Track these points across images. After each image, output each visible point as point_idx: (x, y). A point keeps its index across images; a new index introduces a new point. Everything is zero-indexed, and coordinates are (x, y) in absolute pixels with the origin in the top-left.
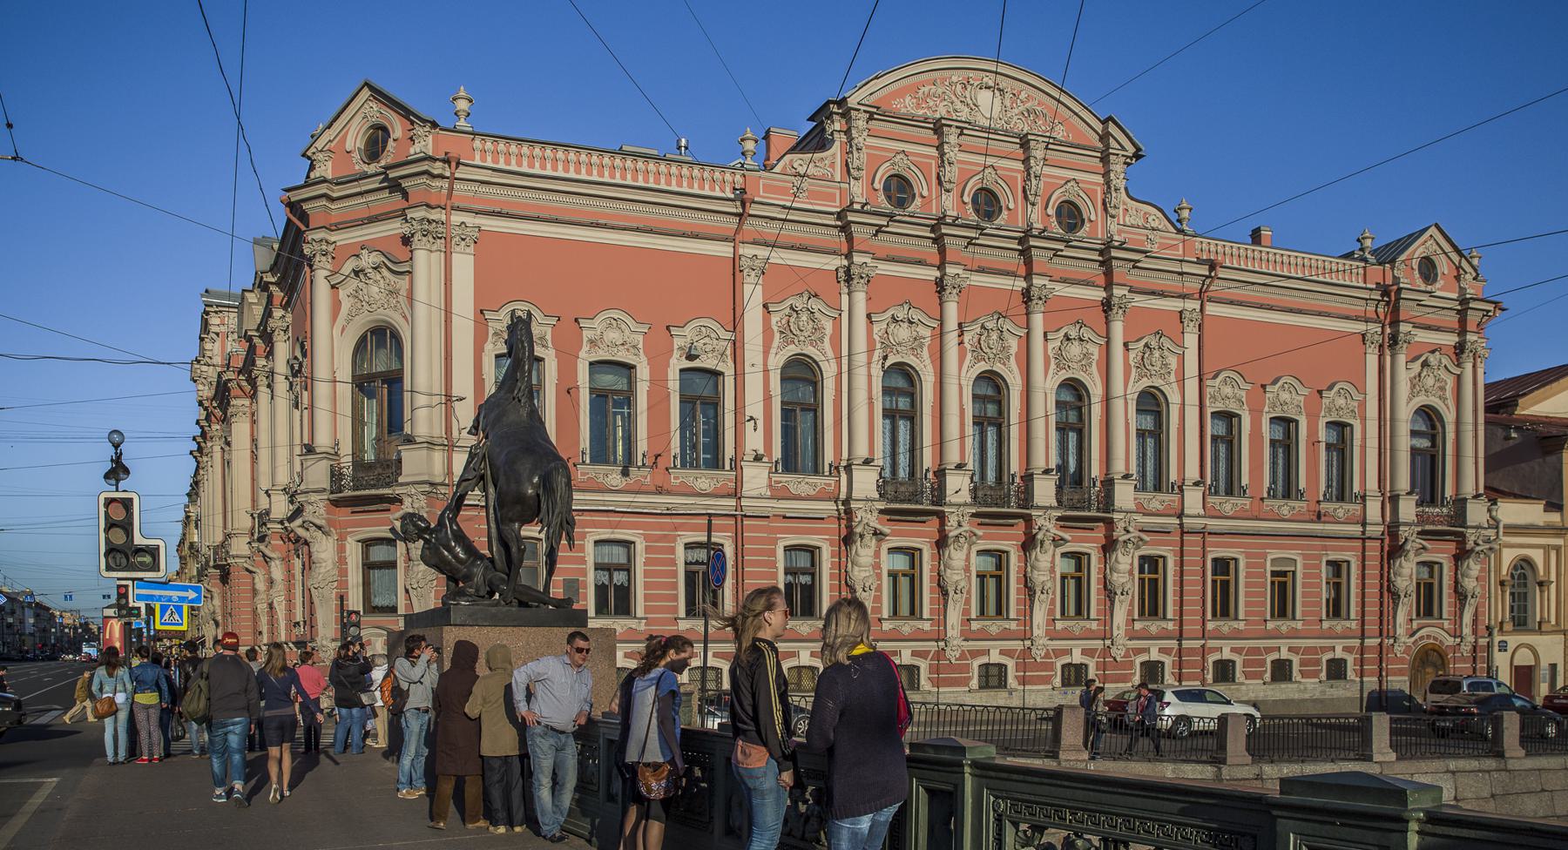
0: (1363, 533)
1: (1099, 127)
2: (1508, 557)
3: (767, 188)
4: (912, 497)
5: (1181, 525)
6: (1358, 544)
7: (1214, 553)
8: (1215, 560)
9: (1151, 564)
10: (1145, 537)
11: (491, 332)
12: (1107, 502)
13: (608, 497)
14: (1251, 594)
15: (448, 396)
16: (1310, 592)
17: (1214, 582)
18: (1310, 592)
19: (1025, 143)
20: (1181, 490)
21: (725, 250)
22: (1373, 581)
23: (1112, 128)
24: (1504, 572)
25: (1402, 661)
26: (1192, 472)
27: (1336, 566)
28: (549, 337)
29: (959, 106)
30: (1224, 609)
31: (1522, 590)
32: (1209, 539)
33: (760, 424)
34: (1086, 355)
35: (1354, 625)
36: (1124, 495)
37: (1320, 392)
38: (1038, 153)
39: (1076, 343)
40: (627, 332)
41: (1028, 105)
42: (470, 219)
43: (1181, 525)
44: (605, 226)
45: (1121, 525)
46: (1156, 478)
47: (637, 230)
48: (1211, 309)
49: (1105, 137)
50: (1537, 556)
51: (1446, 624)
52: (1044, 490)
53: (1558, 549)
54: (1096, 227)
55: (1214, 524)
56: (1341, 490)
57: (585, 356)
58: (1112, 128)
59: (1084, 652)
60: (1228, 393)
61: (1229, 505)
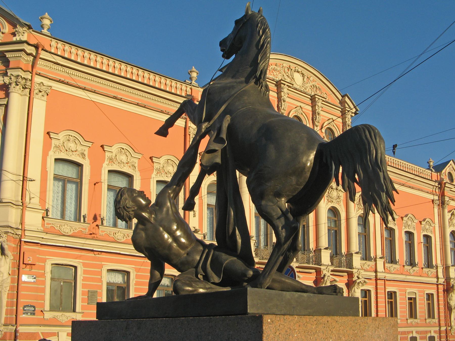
0: (437, 282)
1: (340, 98)
5: (376, 276)
6: (436, 286)
7: (389, 289)
8: (388, 292)
10: (366, 280)
11: (53, 145)
12: (350, 265)
15: (24, 179)
16: (421, 307)
17: (388, 301)
18: (421, 307)
19: (313, 99)
20: (375, 260)
22: (442, 302)
23: (347, 99)
27: (430, 296)
28: (86, 153)
29: (286, 77)
32: (387, 283)
34: (339, 197)
35: (436, 320)
36: (357, 261)
37: (420, 222)
38: (319, 104)
39: (335, 191)
40: (129, 156)
41: (314, 83)
42: (46, 82)
43: (376, 276)
44: (121, 100)
45: (356, 275)
47: (138, 105)
49: (342, 103)
52: (326, 257)
55: (389, 276)
56: (429, 264)
57: (106, 167)
58: (347, 99)
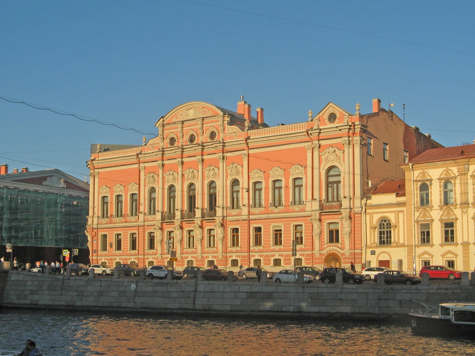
2: (376, 218)
3: (147, 149)
4: (168, 217)
9: (236, 230)
13: (132, 224)
14: (268, 236)
21: (137, 166)
24: (374, 223)
25: (318, 259)
26: (246, 202)
30: (258, 242)
31: (388, 230)
33: (143, 205)
46: (235, 204)
48: (251, 152)
50: (392, 217)
51: (340, 245)
53: (402, 211)
54: (220, 137)
59: (213, 257)
60: (257, 176)
61: (257, 210)
